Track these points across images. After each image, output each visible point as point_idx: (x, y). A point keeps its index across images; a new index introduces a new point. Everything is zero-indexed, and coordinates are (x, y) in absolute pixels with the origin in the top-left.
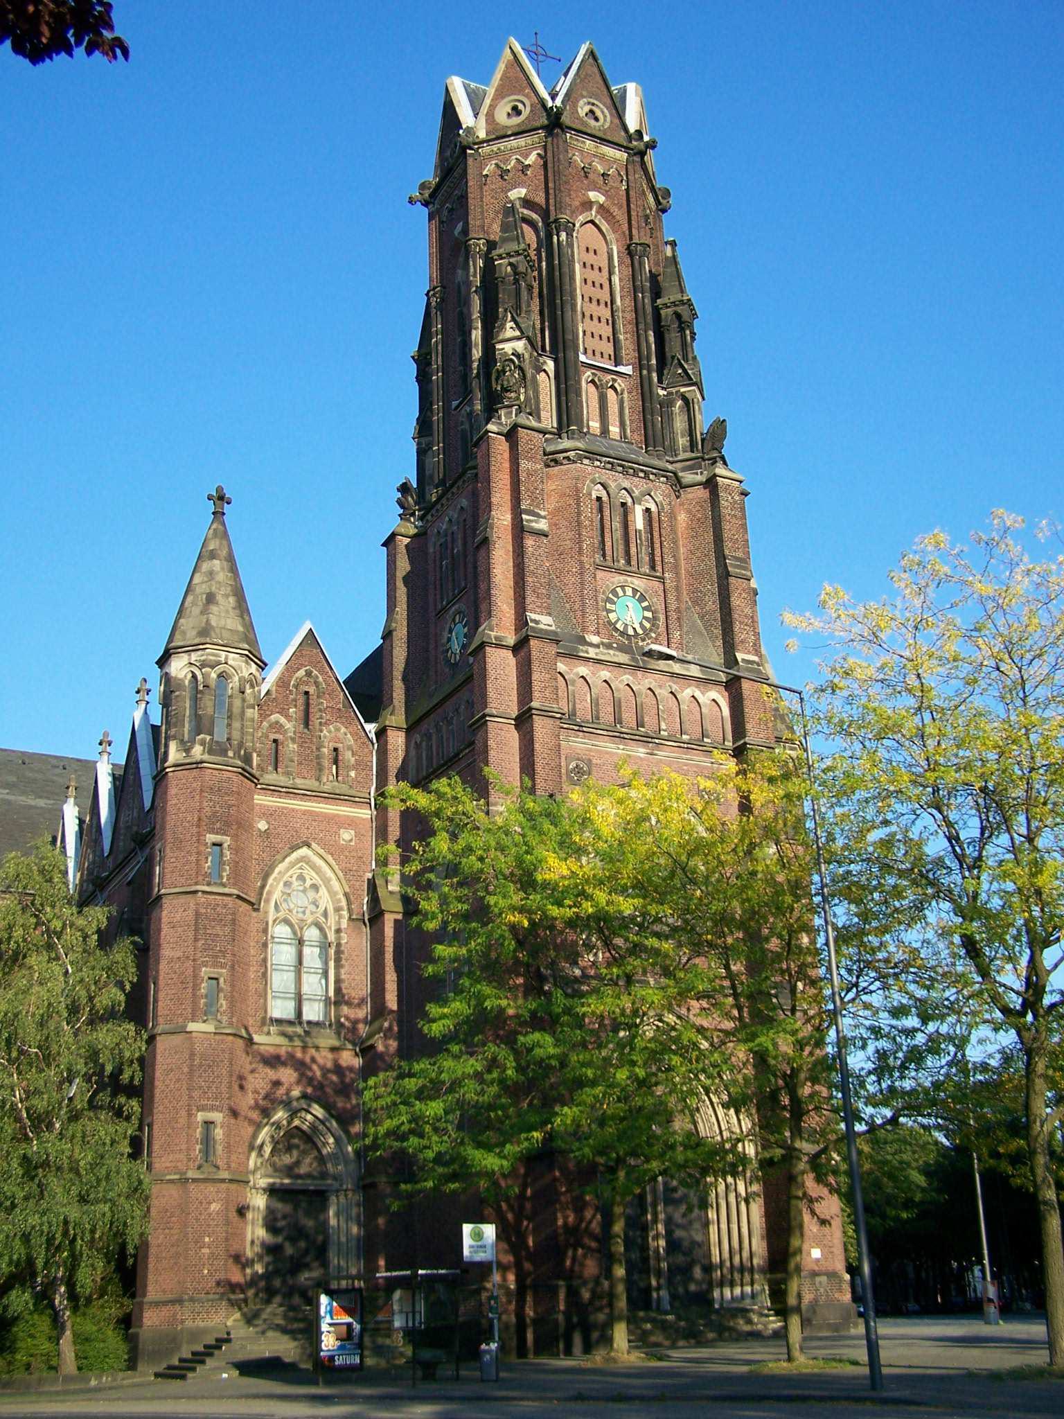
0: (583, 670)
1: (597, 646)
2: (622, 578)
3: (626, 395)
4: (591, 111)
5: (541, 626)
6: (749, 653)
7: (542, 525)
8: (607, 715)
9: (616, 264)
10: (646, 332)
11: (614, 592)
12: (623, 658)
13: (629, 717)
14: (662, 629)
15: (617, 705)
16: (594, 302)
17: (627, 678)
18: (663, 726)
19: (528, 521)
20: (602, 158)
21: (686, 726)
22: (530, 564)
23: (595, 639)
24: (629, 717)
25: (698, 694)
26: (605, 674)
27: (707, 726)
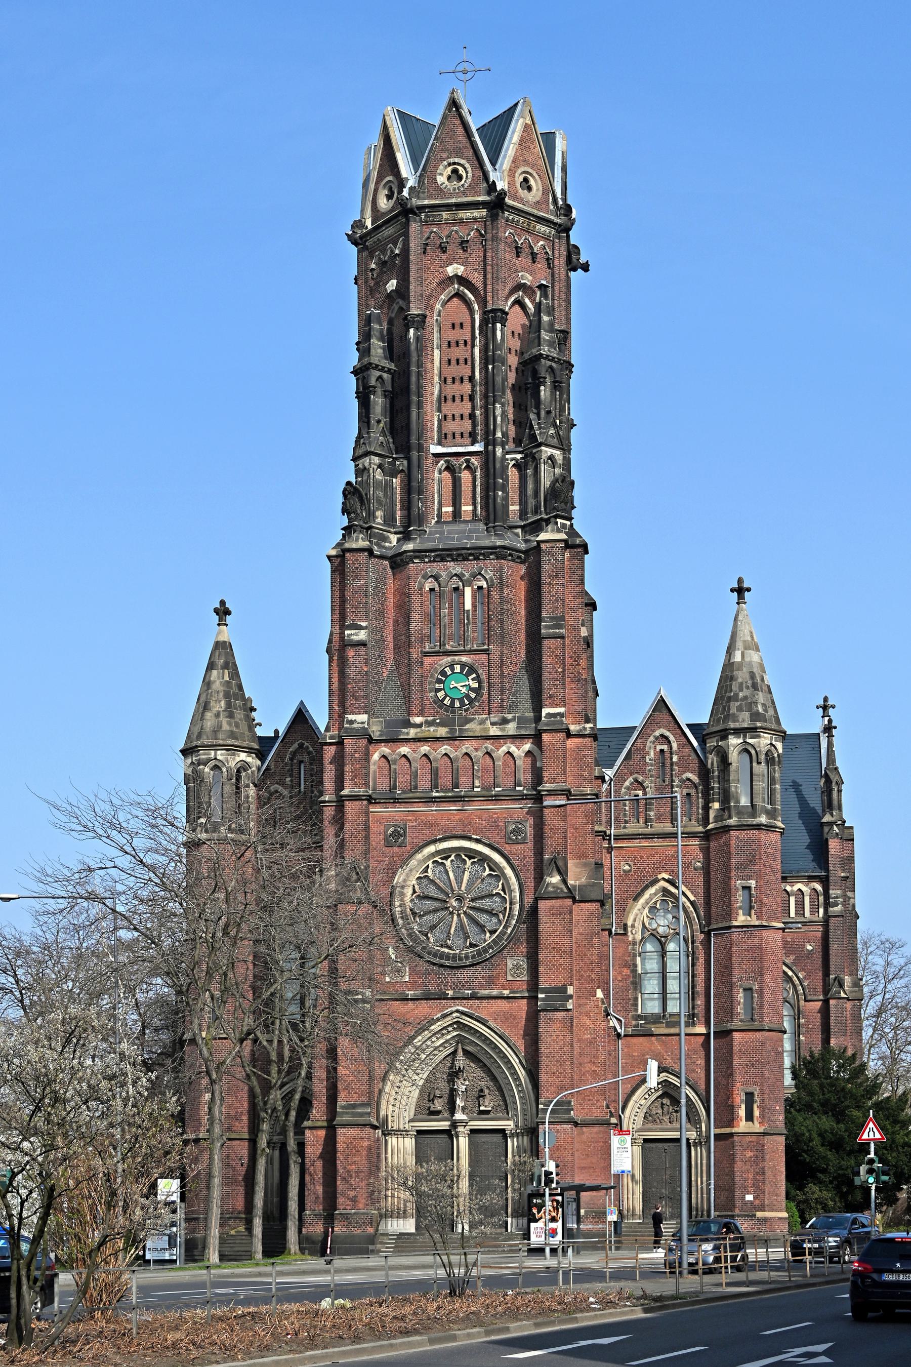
0: (404, 750)
1: (420, 726)
2: (449, 659)
3: (478, 473)
4: (455, 171)
5: (355, 725)
6: (557, 706)
7: (362, 635)
8: (424, 782)
9: (477, 335)
10: (494, 405)
11: (443, 673)
12: (443, 731)
13: (445, 780)
14: (486, 696)
15: (434, 772)
16: (457, 382)
17: (445, 748)
18: (477, 783)
19: (349, 635)
20: (461, 222)
21: (500, 780)
22: (351, 673)
23: (418, 720)
24: (445, 780)
25: (513, 749)
26: (425, 749)
27: (521, 776)
